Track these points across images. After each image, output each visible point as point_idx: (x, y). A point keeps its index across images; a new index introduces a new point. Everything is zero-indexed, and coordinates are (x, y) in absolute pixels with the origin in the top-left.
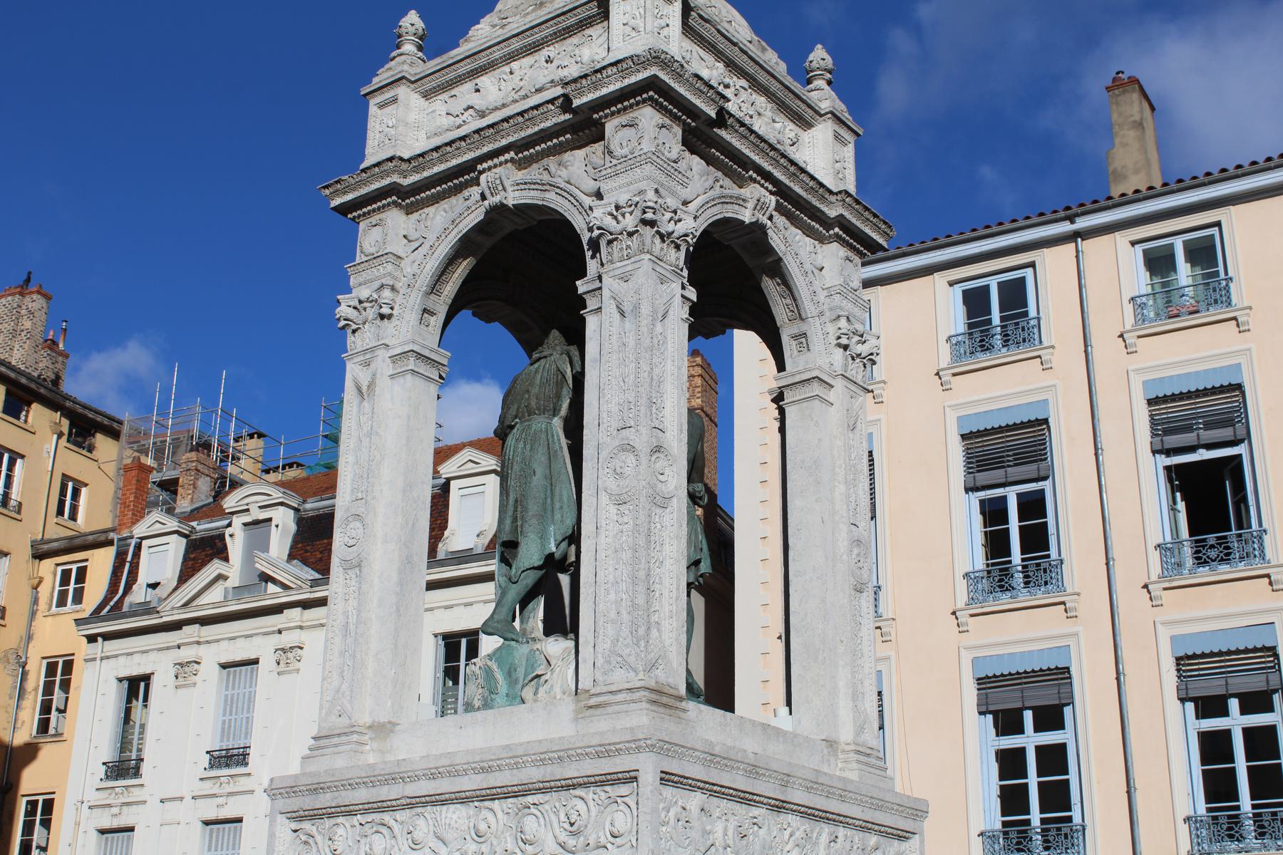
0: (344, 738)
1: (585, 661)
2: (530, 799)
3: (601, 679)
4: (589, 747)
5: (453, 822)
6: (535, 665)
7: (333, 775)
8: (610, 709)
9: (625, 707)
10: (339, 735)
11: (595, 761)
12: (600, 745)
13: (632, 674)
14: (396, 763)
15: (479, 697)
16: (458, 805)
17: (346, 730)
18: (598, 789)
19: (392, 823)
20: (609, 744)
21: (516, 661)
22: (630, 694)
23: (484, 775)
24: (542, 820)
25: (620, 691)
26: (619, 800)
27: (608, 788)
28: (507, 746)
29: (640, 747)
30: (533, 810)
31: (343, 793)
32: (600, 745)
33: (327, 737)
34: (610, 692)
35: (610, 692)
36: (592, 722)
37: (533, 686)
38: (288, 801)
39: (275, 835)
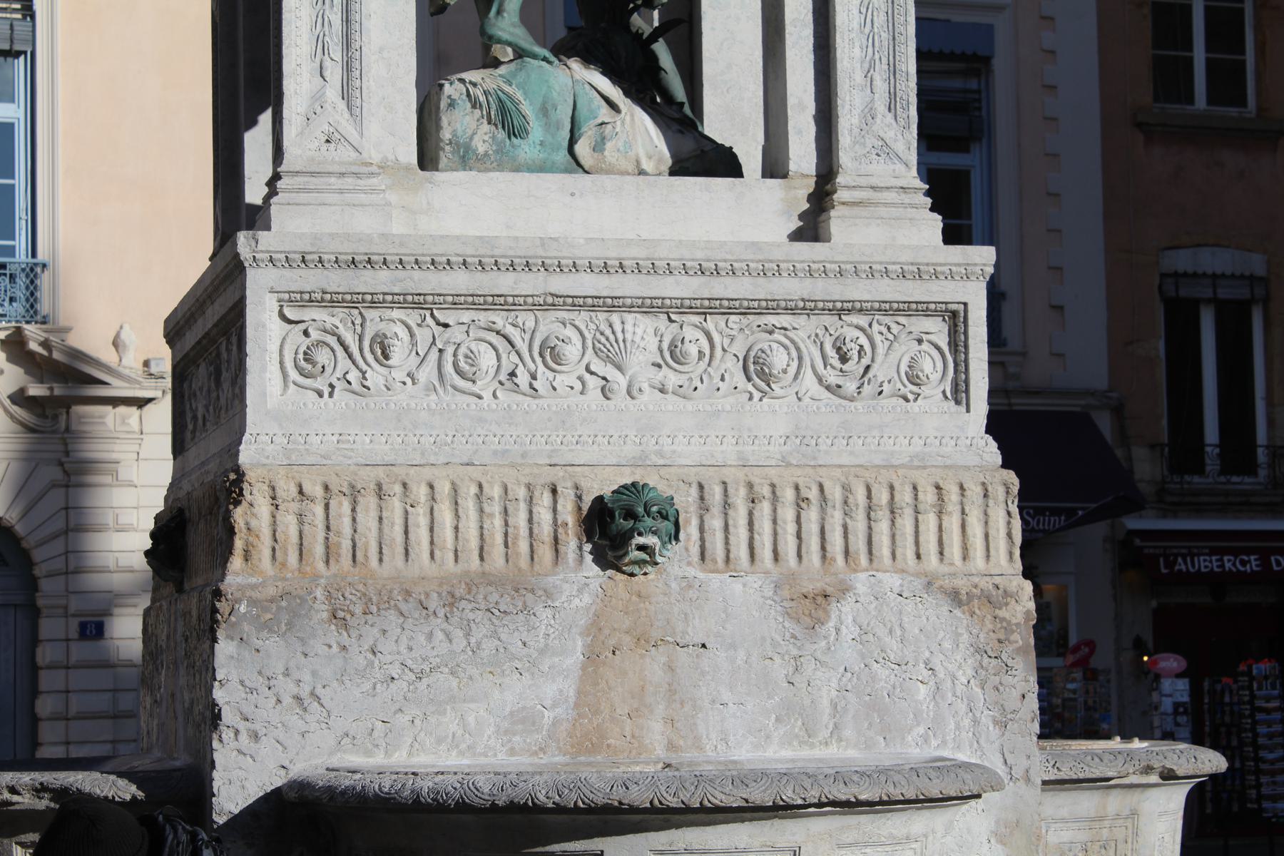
0: (349, 182)
1: (800, 132)
2: (771, 320)
3: (849, 165)
4: (894, 263)
5: (637, 339)
6: (593, 106)
7: (401, 245)
8: (882, 211)
9: (894, 212)
10: (342, 175)
11: (897, 282)
12: (912, 264)
13: (903, 168)
14: (538, 243)
15: (486, 138)
16: (638, 316)
17: (354, 169)
18: (887, 320)
19: (510, 330)
20: (927, 265)
21: (555, 94)
22: (903, 196)
23: (703, 279)
24: (794, 354)
25: (887, 188)
26: (925, 337)
27: (902, 320)
28: (753, 243)
29: (973, 273)
30: (778, 336)
31: (417, 274)
32: (912, 264)
33: (312, 174)
34: (872, 188)
35: (872, 188)
36: (856, 225)
37: (590, 136)
38: (287, 273)
39: (264, 326)
